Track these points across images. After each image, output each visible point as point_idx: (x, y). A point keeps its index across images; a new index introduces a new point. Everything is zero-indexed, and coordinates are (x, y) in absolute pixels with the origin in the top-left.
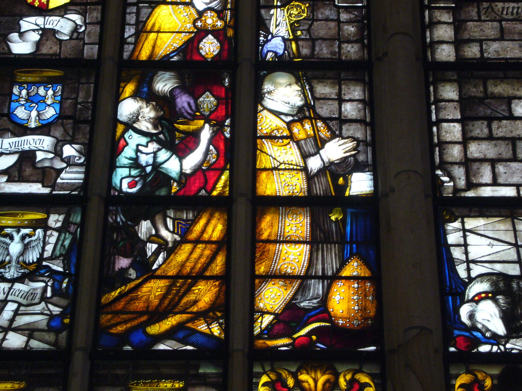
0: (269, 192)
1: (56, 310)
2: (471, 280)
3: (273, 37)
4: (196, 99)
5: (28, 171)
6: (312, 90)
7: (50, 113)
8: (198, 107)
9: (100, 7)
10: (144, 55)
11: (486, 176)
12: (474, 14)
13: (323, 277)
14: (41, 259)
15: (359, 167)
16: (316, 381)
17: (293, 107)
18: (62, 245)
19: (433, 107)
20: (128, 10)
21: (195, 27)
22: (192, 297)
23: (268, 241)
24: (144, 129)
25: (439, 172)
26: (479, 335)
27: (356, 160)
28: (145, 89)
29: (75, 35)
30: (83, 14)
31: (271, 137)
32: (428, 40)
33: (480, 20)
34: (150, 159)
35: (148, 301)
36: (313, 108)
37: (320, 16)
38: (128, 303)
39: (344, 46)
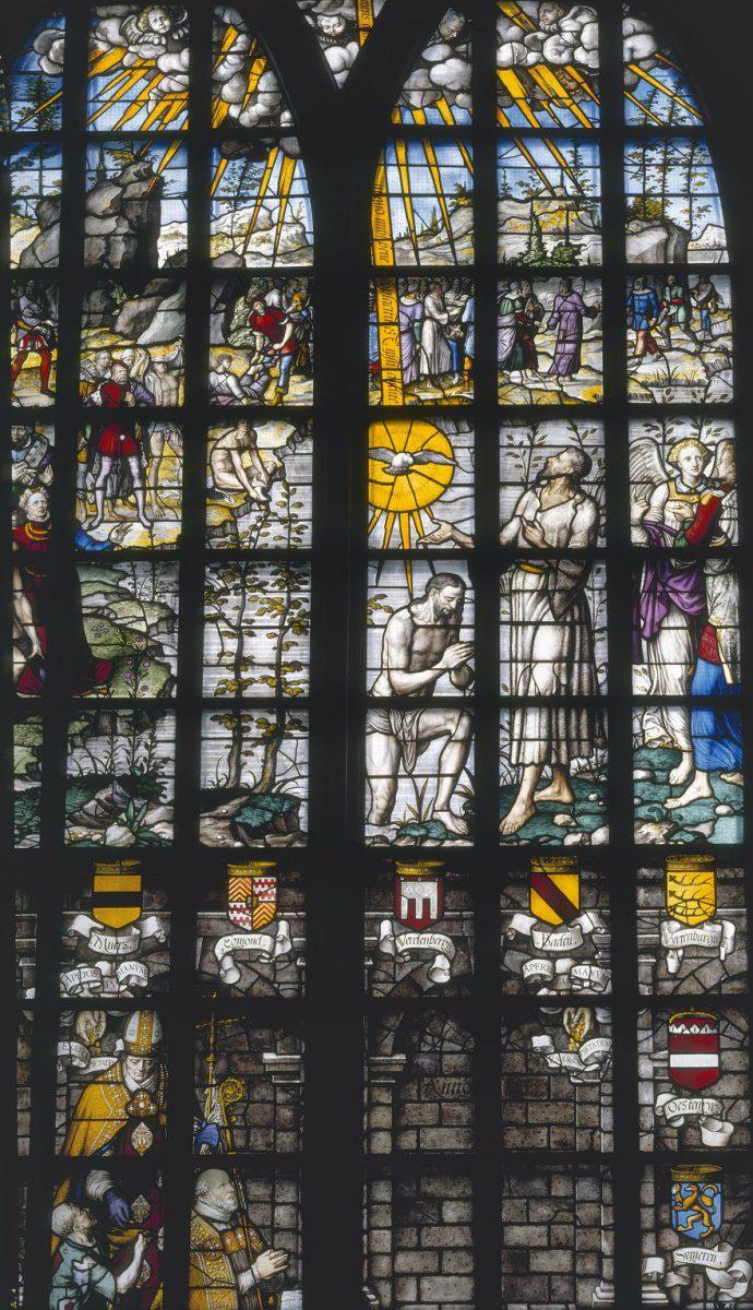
3: (207, 1124)
4: (129, 1205)
8: (131, 1212)
10: (75, 1152)
15: (289, 1284)
17: (226, 1212)
20: (58, 1093)
21: (127, 1113)
24: (79, 1241)
25: (366, 1289)
27: (286, 1276)
28: (79, 1193)
31: (203, 1249)
32: (365, 1127)
33: (419, 1101)
37: (256, 1096)
39: (280, 1134)
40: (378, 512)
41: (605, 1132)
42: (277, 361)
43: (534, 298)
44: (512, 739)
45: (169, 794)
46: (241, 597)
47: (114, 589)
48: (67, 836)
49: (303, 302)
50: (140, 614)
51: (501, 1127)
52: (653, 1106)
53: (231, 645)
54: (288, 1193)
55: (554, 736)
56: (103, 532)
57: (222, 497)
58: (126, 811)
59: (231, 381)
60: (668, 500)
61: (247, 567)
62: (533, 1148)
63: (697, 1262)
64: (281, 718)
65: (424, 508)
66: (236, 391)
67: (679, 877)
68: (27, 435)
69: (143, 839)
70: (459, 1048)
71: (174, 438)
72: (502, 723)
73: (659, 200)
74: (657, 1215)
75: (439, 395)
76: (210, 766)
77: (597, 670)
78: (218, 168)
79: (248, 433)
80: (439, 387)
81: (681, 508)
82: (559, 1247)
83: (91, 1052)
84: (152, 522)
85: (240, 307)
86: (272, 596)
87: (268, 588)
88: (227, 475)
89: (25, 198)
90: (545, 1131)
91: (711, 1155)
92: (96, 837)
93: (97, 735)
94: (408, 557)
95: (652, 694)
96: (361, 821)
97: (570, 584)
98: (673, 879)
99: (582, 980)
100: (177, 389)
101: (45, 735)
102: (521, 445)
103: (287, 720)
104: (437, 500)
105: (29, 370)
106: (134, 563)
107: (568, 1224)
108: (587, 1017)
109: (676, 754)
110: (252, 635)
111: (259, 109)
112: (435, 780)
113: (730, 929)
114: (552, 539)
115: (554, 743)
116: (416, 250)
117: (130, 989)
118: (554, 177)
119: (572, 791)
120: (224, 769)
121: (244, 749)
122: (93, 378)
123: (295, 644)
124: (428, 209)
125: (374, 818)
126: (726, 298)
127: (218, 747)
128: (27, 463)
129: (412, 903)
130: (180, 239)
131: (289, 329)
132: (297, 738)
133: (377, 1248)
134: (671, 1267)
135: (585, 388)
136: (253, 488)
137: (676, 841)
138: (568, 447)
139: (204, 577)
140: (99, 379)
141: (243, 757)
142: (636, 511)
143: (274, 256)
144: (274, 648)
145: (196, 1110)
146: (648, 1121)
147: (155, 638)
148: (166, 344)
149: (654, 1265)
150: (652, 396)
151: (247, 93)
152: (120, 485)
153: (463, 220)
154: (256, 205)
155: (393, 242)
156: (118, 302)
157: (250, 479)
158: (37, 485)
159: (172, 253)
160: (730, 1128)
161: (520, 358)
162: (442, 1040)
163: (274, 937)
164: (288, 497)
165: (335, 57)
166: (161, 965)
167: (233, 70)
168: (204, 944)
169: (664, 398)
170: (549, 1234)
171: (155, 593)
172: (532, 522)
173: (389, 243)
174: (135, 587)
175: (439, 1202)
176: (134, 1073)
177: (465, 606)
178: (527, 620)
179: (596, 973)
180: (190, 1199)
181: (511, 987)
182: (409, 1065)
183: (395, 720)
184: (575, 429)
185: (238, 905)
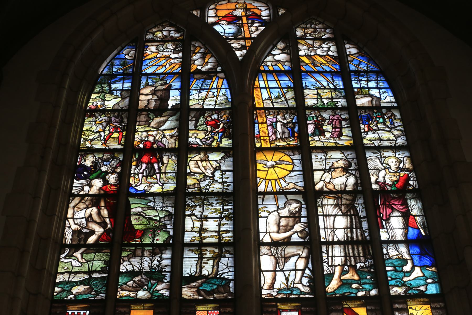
40: (261, 180)
42: (217, 134)
43: (321, 116)
44: (328, 257)
46: (202, 208)
47: (145, 206)
48: (118, 294)
49: (227, 117)
50: (157, 214)
53: (198, 224)
55: (348, 255)
56: (141, 188)
57: (194, 175)
58: (147, 285)
59: (198, 141)
60: (386, 175)
61: (204, 198)
64: (221, 250)
65: (281, 178)
66: (200, 143)
67: (414, 307)
68: (111, 157)
69: (155, 296)
71: (173, 158)
72: (323, 250)
75: (285, 144)
76: (187, 268)
77: (364, 232)
78: (193, 82)
79: (205, 156)
80: (285, 141)
81: (392, 177)
84: (163, 184)
85: (201, 119)
86: (216, 207)
88: (196, 169)
89: (116, 90)
92: (133, 295)
95: (390, 239)
96: (261, 288)
97: (348, 202)
98: (411, 308)
100: (175, 143)
101: (111, 257)
102: (321, 159)
103: (224, 250)
104: (287, 176)
105: (114, 138)
106: (155, 197)
109: (405, 262)
110: (207, 221)
111: (209, 66)
112: (294, 272)
114: (338, 188)
115: (348, 258)
116: (272, 103)
118: (325, 84)
119: (358, 275)
120: (194, 269)
121: (203, 262)
122: (140, 140)
123: (226, 224)
124: (276, 93)
125: (266, 287)
126: (398, 116)
127: (191, 261)
128: (110, 165)
130: (177, 101)
131: (221, 125)
132: (228, 257)
135: (345, 141)
136: (207, 173)
137: (410, 293)
138: (341, 159)
139: (185, 201)
140: (142, 141)
141: (203, 265)
142: (373, 179)
143: (215, 105)
144: (217, 225)
147: (163, 222)
148: (171, 129)
150: (374, 143)
151: (204, 63)
152: (150, 172)
153: (290, 95)
154: (208, 91)
155: (263, 101)
156: (152, 118)
157: (206, 170)
158: (113, 172)
159: (174, 104)
161: (318, 133)
164: (222, 175)
165: (238, 53)
167: (199, 57)
169: (378, 144)
171: (163, 207)
172: (329, 182)
173: (262, 101)
174: (155, 205)
177: (302, 210)
178: (330, 214)
183: (274, 250)
184: (343, 154)
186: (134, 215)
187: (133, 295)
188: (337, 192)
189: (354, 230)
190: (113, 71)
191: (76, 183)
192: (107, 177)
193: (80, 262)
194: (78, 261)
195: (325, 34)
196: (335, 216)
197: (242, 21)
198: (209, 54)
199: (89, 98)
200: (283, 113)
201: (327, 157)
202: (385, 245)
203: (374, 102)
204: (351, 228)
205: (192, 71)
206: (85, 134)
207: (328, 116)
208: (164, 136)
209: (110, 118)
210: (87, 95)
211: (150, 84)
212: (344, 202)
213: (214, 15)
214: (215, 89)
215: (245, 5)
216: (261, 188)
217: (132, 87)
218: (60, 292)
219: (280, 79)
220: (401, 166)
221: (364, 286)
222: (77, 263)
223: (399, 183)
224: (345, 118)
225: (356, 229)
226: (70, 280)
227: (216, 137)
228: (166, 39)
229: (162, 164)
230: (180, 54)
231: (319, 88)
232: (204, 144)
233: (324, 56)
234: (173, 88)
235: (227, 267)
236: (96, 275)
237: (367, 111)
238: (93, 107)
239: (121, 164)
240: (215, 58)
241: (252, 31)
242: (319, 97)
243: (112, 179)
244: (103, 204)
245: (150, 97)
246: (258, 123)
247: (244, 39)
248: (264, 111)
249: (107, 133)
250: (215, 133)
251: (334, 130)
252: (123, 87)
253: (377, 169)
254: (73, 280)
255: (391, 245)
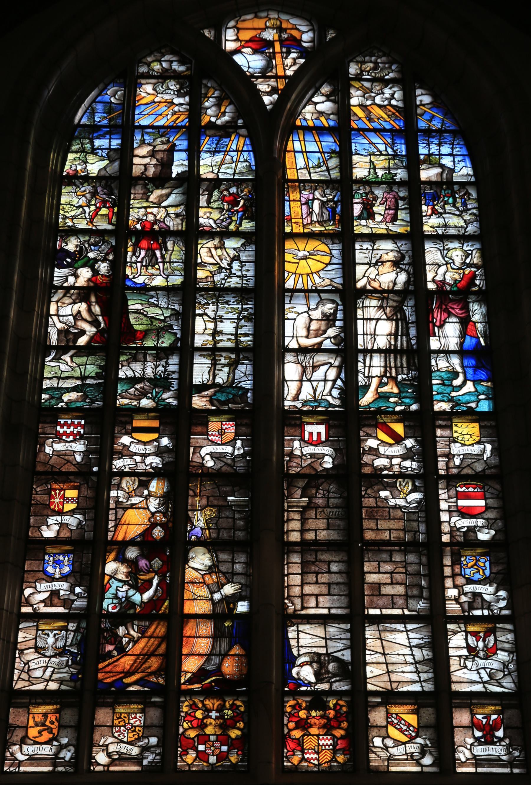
0: (191, 612)
1: (74, 671)
2: (299, 655)
3: (195, 527)
5: (56, 601)
6: (217, 556)
7: (66, 570)
8: (151, 566)
9: (93, 511)
11: (313, 603)
12: (313, 515)
13: (220, 655)
14: (65, 646)
15: (242, 599)
16: (213, 705)
17: (206, 566)
18: (76, 639)
19: (286, 566)
21: (149, 521)
22: (147, 665)
23: (190, 637)
24: (120, 578)
25: (286, 601)
26: (301, 682)
27: (240, 595)
29: (80, 526)
30: (84, 514)
31: (192, 582)
32: (286, 530)
33: (316, 518)
34: (124, 594)
35: (124, 666)
36: (217, 566)
37: (223, 515)
38: (113, 667)
39: (237, 532)
40: (290, 274)
41: (422, 534)
43: (373, 193)
44: (365, 367)
45: (175, 384)
49: (249, 192)
50: (161, 312)
51: (362, 531)
52: (449, 522)
53: (211, 326)
54: (242, 558)
56: (140, 280)
57: (206, 267)
58: (151, 393)
62: (381, 540)
63: (477, 591)
64: (238, 356)
65: (315, 273)
67: (459, 425)
70: (338, 496)
73: (438, 157)
74: (453, 570)
75: (323, 229)
79: (220, 242)
80: (323, 226)
82: (398, 583)
83: (129, 495)
84: (168, 276)
85: (216, 193)
86: (233, 306)
87: (231, 303)
89: (101, 149)
90: (388, 532)
91: (483, 544)
93: (136, 361)
94: (306, 292)
96: (283, 399)
97: (395, 304)
98: (456, 425)
99: (407, 468)
100: (182, 224)
101: (107, 361)
102: (367, 249)
103: (241, 357)
104: (323, 270)
105: (102, 215)
107: (402, 573)
108: (410, 484)
109: (456, 375)
110: (222, 322)
111: (226, 118)
112: (323, 383)
113: (489, 447)
114: (385, 286)
115: (388, 369)
116: (310, 173)
117: (152, 468)
118: (382, 147)
119: (399, 388)
120: (206, 377)
124: (315, 159)
125: (289, 398)
126: (474, 195)
127: (203, 367)
129: (311, 434)
131: (242, 202)
133: (293, 583)
134: (462, 593)
138: (392, 250)
139: (196, 298)
140: (139, 220)
141: (217, 372)
142: (430, 276)
143: (234, 174)
145: (189, 520)
146: (446, 528)
148: (176, 206)
149: (452, 592)
150: (436, 231)
152: (150, 261)
153: (333, 163)
155: (297, 170)
157: (221, 260)
158: (104, 260)
159: (180, 172)
160: (493, 532)
161: (365, 215)
162: (329, 492)
163: (234, 447)
164: (242, 267)
165: (267, 99)
166: (169, 458)
167: (212, 104)
168: (194, 449)
170: (391, 578)
171: (169, 304)
174: (158, 301)
175: (329, 563)
176: (153, 504)
178: (372, 317)
179: (415, 465)
180: (186, 561)
181: (367, 470)
182: (309, 503)
183: (301, 358)
184: (396, 243)
185: (214, 433)
186: (133, 312)
187: (135, 403)
188: (383, 291)
189: (399, 338)
190: (94, 121)
191: (58, 273)
192: (97, 266)
193: (70, 366)
194: (67, 365)
195: (389, 73)
196: (378, 320)
197: (274, 49)
198: (227, 99)
199: (65, 159)
200: (323, 188)
201: (375, 247)
202: (433, 355)
203: (445, 175)
204: (396, 335)
205: (203, 124)
206: (63, 208)
207: (381, 193)
208: (168, 215)
209: (94, 187)
210: (61, 154)
211: (147, 142)
212: (391, 303)
213: (234, 38)
214: (234, 151)
215: (279, 23)
216: (289, 284)
217: (122, 145)
218: (49, 399)
219: (321, 139)
220: (468, 261)
221: (404, 400)
222: (67, 367)
223: (462, 282)
224: (404, 197)
225: (402, 336)
226: (59, 386)
227: (234, 218)
228: (166, 74)
229: (165, 251)
230: (187, 99)
231: (373, 154)
232: (219, 227)
233: (385, 106)
234: (177, 148)
235: (245, 375)
236: (90, 381)
237: (434, 187)
238: (71, 172)
239: (114, 249)
240: (235, 106)
241: (287, 66)
242: (373, 167)
243: (103, 268)
244: (93, 299)
245: (147, 160)
246: (289, 201)
247: (276, 77)
248: (297, 184)
249: (93, 208)
250: (233, 212)
251: (387, 212)
252: (110, 145)
253: (437, 264)
254: (63, 386)
255: (442, 355)
